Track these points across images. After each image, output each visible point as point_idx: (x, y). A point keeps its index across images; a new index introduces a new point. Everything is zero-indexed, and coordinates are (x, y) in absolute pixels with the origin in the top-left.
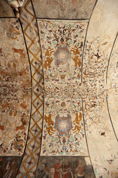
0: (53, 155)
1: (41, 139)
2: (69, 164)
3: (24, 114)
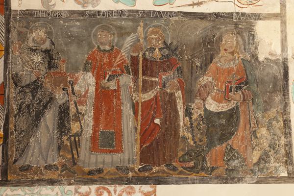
0: (80, 8)
2: (166, 52)
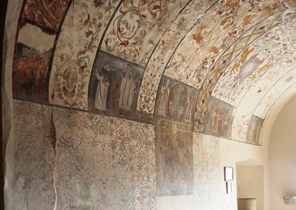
1: (221, 74)
3: (235, 32)
